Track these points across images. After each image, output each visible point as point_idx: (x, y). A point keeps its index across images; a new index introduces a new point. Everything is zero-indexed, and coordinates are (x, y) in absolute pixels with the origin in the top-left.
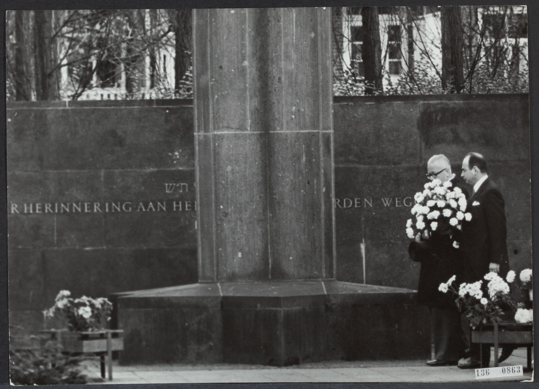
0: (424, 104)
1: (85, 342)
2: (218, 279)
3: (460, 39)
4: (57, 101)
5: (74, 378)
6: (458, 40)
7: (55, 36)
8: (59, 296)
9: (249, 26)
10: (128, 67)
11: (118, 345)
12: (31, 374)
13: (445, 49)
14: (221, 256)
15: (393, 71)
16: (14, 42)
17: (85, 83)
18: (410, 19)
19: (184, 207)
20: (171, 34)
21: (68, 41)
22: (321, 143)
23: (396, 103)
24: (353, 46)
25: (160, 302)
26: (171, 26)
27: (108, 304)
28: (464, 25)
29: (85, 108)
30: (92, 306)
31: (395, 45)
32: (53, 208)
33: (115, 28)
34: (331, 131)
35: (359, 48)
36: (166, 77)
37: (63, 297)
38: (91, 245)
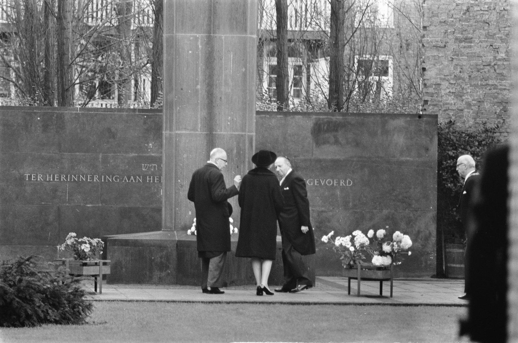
0: (316, 118)
1: (85, 268)
2: (175, 229)
3: (341, 76)
5: (77, 291)
6: (341, 76)
7: (71, 63)
8: (68, 236)
9: (201, 62)
10: (120, 86)
11: (107, 270)
12: (48, 288)
13: (331, 82)
14: (178, 213)
15: (296, 95)
16: (44, 67)
17: (91, 96)
18: (309, 61)
20: (148, 65)
21: (80, 68)
23: (297, 117)
24: (270, 77)
25: (135, 243)
26: (149, 60)
27: (101, 243)
28: (345, 66)
29: (90, 112)
30: (90, 244)
31: (299, 78)
33: (111, 60)
34: (254, 134)
35: (274, 79)
36: (144, 94)
38: (91, 203)
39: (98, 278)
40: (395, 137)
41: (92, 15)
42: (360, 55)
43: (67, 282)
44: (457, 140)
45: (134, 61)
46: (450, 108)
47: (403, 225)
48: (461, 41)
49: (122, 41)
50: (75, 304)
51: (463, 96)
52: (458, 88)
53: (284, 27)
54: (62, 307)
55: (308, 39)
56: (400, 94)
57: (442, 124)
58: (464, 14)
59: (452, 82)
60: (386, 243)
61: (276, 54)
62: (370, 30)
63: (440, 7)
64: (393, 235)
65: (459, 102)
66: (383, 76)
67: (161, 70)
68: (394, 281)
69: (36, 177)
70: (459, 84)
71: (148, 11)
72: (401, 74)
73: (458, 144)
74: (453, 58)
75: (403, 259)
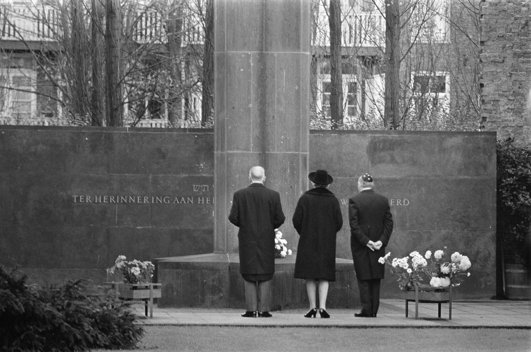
0: (371, 136)
1: (134, 291)
2: (227, 251)
3: (397, 93)
4: (121, 127)
5: (127, 316)
6: (396, 93)
8: (118, 259)
10: (169, 105)
11: (158, 294)
12: (98, 312)
13: (386, 99)
14: (230, 235)
16: (92, 86)
17: (140, 115)
19: (205, 202)
20: (199, 84)
21: (129, 86)
22: (301, 161)
23: (352, 135)
24: (324, 95)
25: (187, 266)
26: (199, 78)
27: (152, 266)
30: (140, 267)
31: (353, 96)
32: (116, 199)
34: (308, 153)
35: (328, 97)
37: (121, 260)
38: (141, 225)
39: (149, 302)
40: (453, 155)
41: (141, 33)
42: (415, 71)
43: (116, 305)
44: (516, 158)
45: (184, 79)
46: (509, 125)
47: (461, 246)
48: (519, 56)
49: (171, 59)
50: (126, 329)
51: (523, 112)
52: (517, 104)
53: (338, 44)
54: (111, 332)
55: (363, 55)
56: (458, 111)
57: (501, 142)
58: (523, 28)
59: (511, 98)
60: (444, 264)
61: (330, 71)
62: (427, 45)
63: (498, 21)
64: (451, 256)
65: (518, 119)
66: (441, 92)
67: (212, 89)
68: (452, 303)
69: (85, 198)
70: (518, 101)
71: (198, 28)
72: (459, 90)
73: (517, 161)
74: (511, 74)
75: (462, 280)
